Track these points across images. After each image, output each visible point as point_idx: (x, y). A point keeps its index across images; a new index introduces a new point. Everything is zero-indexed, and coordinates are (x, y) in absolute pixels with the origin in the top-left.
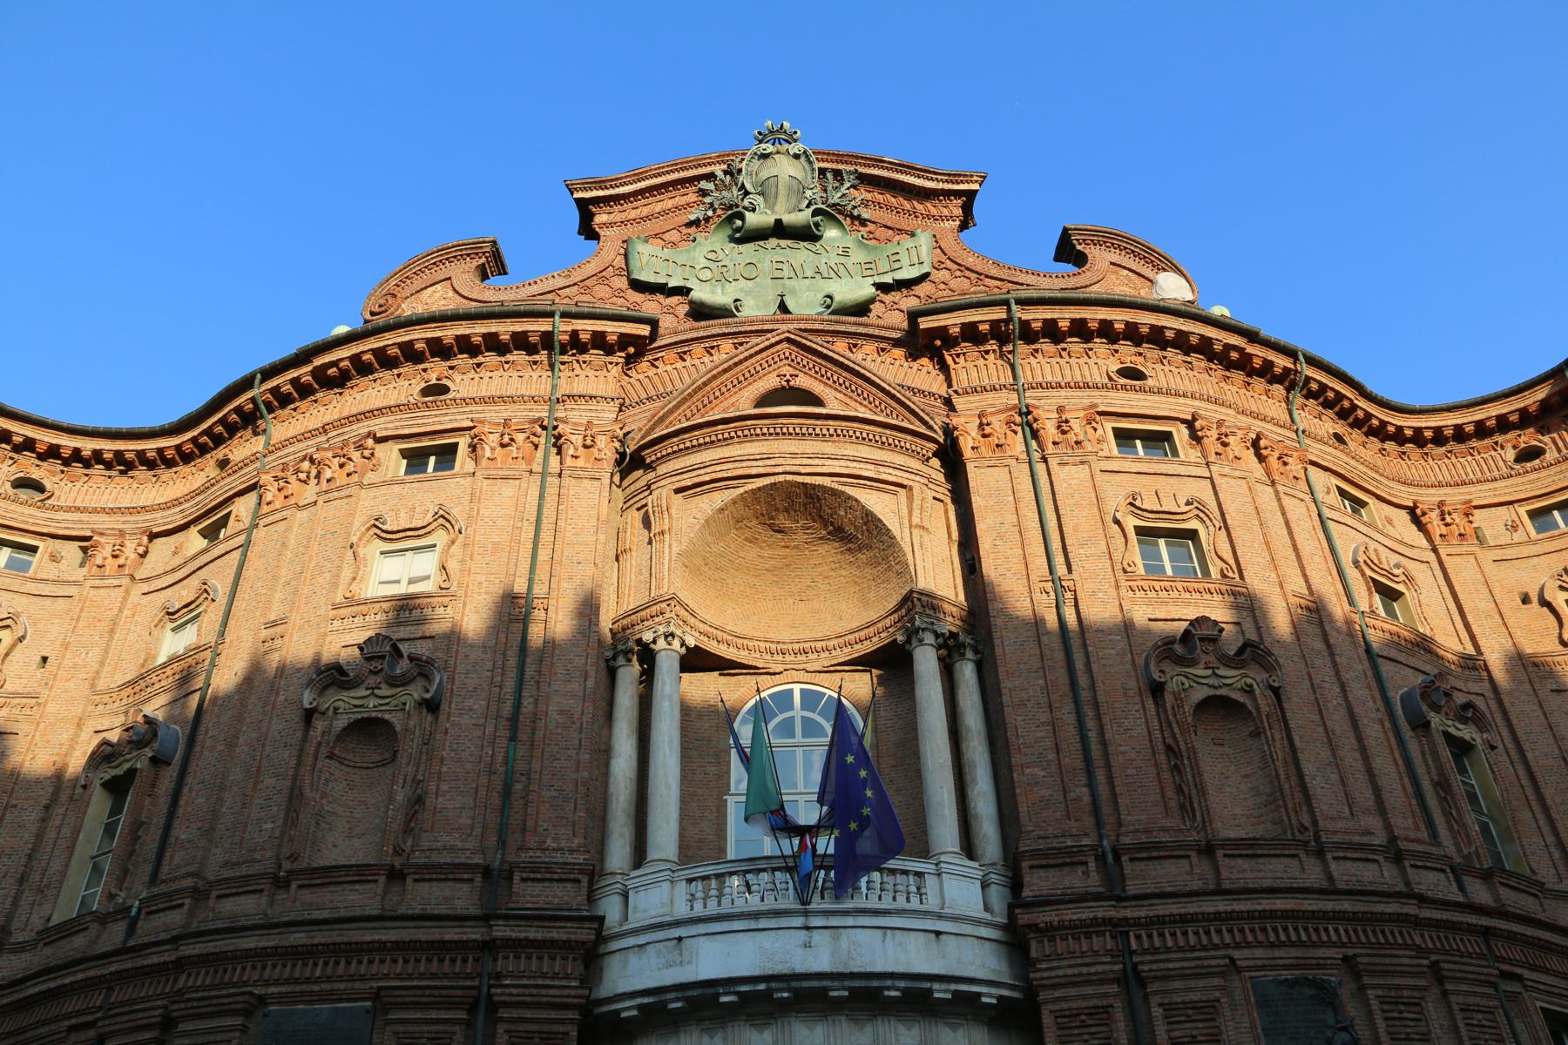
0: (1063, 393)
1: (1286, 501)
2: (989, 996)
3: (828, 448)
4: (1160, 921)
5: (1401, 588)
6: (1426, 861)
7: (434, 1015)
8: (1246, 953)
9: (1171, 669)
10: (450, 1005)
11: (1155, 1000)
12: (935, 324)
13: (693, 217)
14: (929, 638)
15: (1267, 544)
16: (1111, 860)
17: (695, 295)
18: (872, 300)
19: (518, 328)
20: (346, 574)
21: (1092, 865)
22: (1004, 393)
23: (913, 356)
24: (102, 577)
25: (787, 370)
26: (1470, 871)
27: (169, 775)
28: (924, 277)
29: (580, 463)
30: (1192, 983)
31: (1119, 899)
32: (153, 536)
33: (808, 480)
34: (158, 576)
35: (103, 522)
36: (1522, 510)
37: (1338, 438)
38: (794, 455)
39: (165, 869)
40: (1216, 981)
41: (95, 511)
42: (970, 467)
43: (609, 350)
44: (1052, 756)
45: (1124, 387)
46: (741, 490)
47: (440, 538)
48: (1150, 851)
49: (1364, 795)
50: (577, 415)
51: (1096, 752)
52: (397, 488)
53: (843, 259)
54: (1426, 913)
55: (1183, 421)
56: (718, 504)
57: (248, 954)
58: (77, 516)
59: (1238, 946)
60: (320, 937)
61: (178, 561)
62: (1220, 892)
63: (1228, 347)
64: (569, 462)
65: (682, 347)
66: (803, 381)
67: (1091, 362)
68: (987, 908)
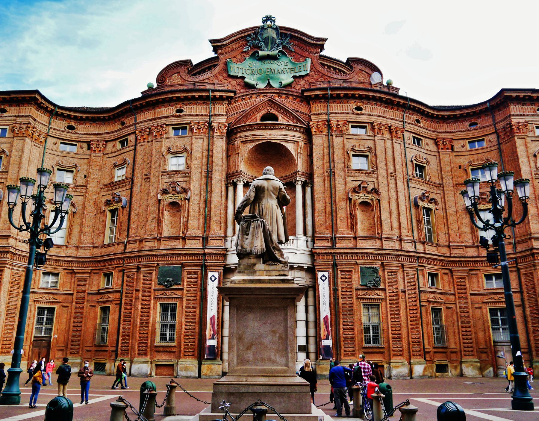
0: (339, 115)
1: (395, 145)
2: (305, 266)
3: (279, 132)
5: (425, 165)
6: (407, 241)
7: (194, 268)
8: (360, 261)
9: (354, 195)
10: (197, 266)
11: (339, 270)
12: (308, 94)
13: (244, 50)
14: (300, 183)
15: (386, 159)
16: (333, 240)
17: (246, 80)
18: (292, 82)
19: (200, 94)
20: (162, 163)
21: (330, 240)
22: (324, 115)
23: (302, 101)
24: (96, 154)
25: (269, 108)
26: (419, 242)
27: (126, 210)
28: (307, 75)
29: (218, 134)
30: (347, 267)
31: (334, 248)
32: (107, 142)
33: (273, 141)
34: (110, 153)
35: (92, 137)
36: (467, 141)
37: (418, 121)
38: (270, 135)
39: (130, 234)
40: (352, 267)
41: (89, 134)
42: (313, 137)
44: (324, 214)
45: (356, 114)
46: (257, 143)
47: (185, 154)
48: (343, 238)
49: (395, 224)
50: (216, 120)
51: (334, 214)
52: (173, 139)
53: (285, 67)
54: (403, 253)
55: (370, 123)
56: (251, 147)
57: (154, 255)
58: (85, 136)
59: (358, 260)
60: (169, 252)
61: (114, 150)
62: (356, 248)
63: (387, 99)
64: (215, 134)
65: (243, 98)
66: (273, 111)
67: (348, 105)
68: (307, 247)
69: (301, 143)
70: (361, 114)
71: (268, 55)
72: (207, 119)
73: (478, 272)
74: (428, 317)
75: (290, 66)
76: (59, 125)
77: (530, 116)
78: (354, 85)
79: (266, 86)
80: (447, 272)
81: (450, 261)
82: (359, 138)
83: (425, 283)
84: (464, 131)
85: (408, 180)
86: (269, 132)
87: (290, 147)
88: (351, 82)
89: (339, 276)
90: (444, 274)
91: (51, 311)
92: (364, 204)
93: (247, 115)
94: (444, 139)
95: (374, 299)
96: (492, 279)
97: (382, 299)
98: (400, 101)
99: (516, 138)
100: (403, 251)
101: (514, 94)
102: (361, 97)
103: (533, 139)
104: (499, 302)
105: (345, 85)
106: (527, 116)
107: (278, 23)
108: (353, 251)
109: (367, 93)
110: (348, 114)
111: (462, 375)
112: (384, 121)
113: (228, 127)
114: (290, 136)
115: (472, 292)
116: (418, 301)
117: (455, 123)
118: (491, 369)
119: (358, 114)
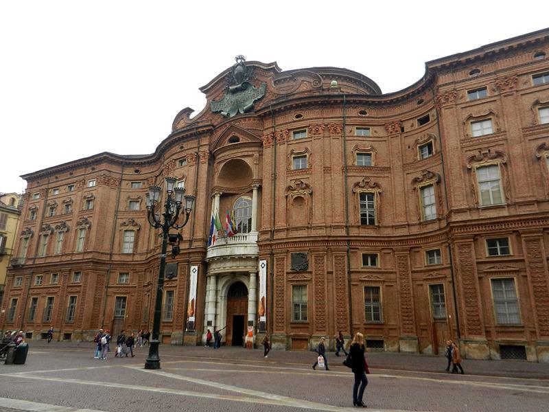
3: (239, 151)
4: (278, 244)
5: (371, 152)
14: (255, 188)
16: (273, 232)
32: (156, 177)
43: (207, 133)
47: (184, 180)
50: (202, 149)
54: (330, 239)
66: (237, 134)
69: (257, 155)
70: (303, 120)
71: (236, 88)
72: (196, 150)
73: (420, 249)
74: (360, 295)
75: (252, 93)
76: (129, 171)
77: (461, 82)
78: (296, 97)
79: (237, 114)
80: (389, 251)
81: (391, 241)
82: (299, 142)
83: (357, 263)
84: (411, 111)
85: (346, 169)
86: (232, 152)
87: (248, 160)
88: (294, 95)
89: (275, 262)
90: (385, 253)
91: (125, 299)
92: (299, 199)
93: (219, 141)
94: (393, 122)
95: (301, 281)
96: (434, 256)
97: (309, 280)
98: (337, 99)
99: (443, 110)
100: (329, 237)
101: (439, 65)
102: (298, 107)
103: (463, 106)
104: (436, 279)
105: (290, 98)
106: (455, 83)
107: (246, 61)
108: (284, 241)
109: (303, 102)
110: (289, 123)
111: (399, 350)
112: (319, 122)
113: (210, 153)
114: (247, 151)
115: (414, 269)
116: (347, 281)
117: (405, 104)
118: (430, 347)
119: (299, 121)
